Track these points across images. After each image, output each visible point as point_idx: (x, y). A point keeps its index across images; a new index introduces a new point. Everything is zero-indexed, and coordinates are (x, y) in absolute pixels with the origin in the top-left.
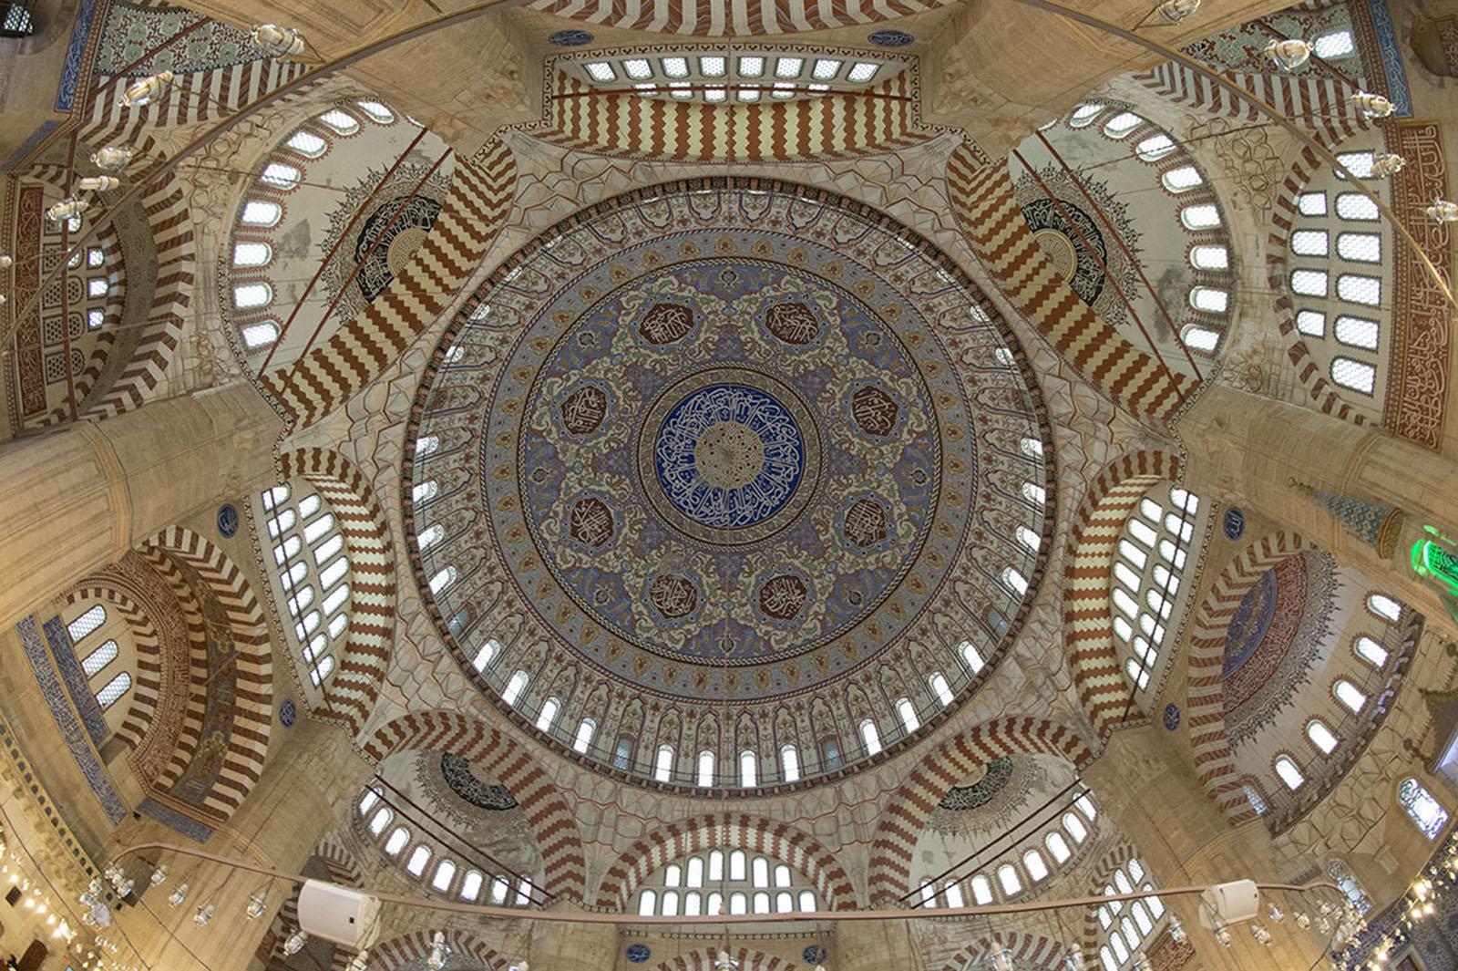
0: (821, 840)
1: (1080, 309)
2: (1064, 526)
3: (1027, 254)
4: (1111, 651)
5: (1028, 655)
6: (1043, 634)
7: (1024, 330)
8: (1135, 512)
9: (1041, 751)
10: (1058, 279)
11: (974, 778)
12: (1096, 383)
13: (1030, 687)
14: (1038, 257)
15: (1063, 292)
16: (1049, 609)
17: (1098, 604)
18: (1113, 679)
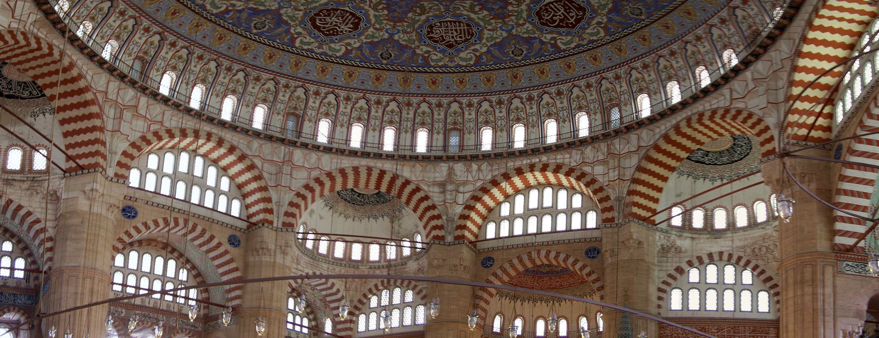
0: (265, 175)
1: (684, 155)
2: (544, 158)
3: (716, 132)
4: (490, 210)
5: (458, 173)
6: (474, 173)
7: (664, 126)
8: (571, 192)
9: (415, 210)
10: (699, 142)
11: (372, 193)
12: (640, 169)
13: (442, 185)
14: (715, 136)
15: (694, 146)
16: (489, 168)
17: (510, 190)
18: (479, 220)
